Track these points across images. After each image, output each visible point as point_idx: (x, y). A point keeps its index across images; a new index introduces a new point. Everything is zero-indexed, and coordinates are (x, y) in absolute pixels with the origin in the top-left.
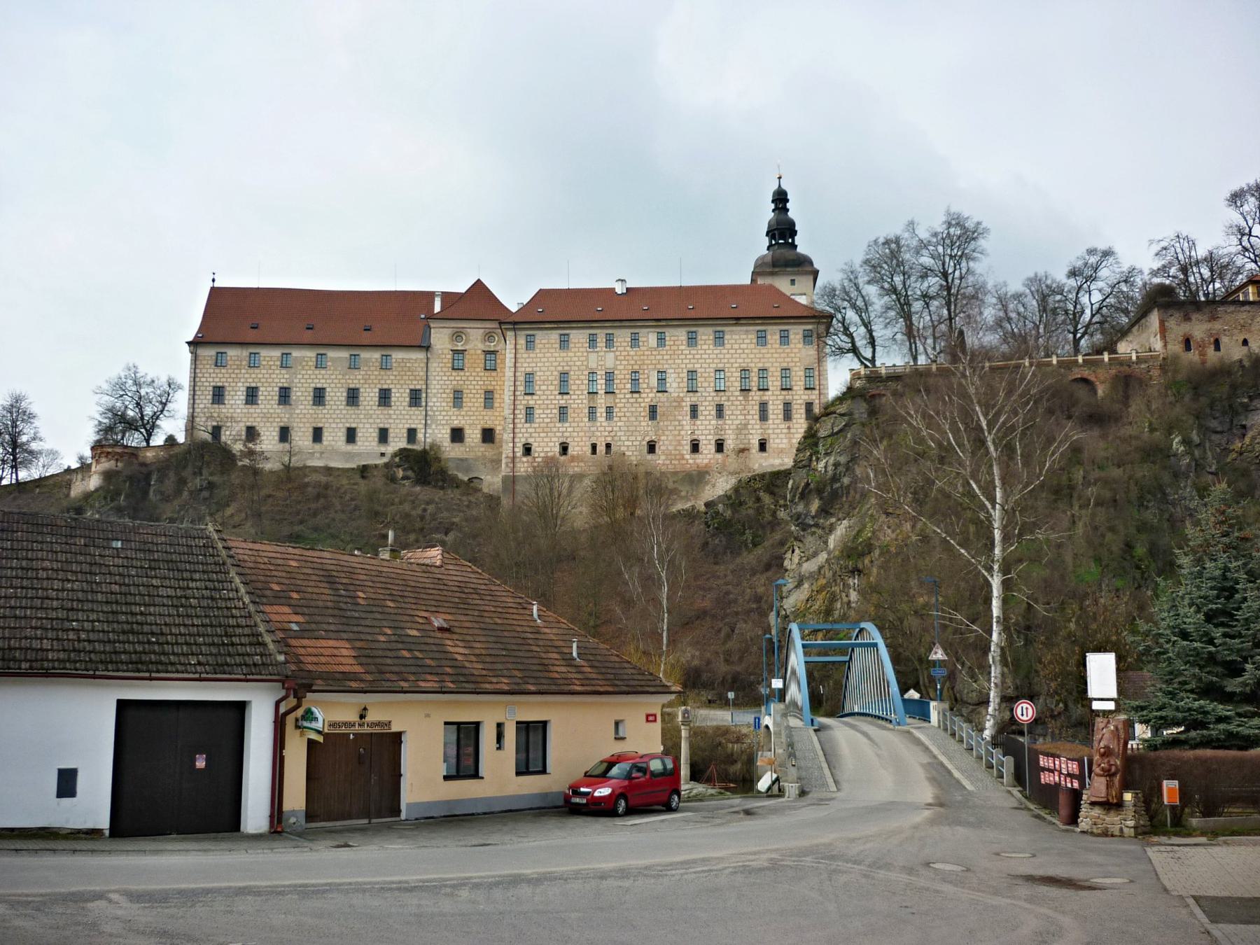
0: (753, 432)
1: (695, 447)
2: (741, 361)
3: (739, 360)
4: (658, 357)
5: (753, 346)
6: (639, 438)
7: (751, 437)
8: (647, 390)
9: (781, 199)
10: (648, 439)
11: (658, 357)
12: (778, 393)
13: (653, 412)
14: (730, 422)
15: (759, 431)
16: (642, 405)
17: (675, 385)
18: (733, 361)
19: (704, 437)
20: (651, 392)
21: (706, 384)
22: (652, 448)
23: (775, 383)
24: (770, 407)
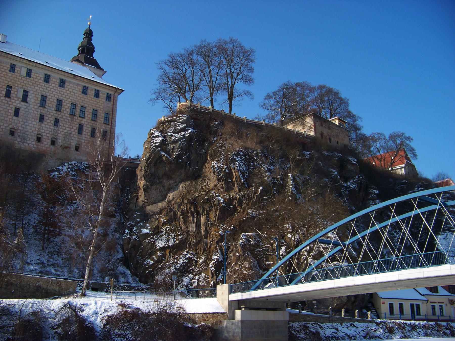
0: (74, 139)
1: (39, 140)
2: (73, 99)
3: (71, 98)
4: (25, 82)
5: (80, 93)
6: (5, 125)
7: (72, 141)
8: (15, 99)
9: (89, 34)
10: (11, 126)
11: (25, 82)
12: (90, 121)
13: (17, 112)
14: (61, 130)
15: (77, 139)
16: (11, 106)
17: (33, 100)
18: (68, 97)
19: (45, 134)
20: (18, 100)
21: (51, 105)
22: (12, 133)
23: (89, 116)
24: (85, 128)
